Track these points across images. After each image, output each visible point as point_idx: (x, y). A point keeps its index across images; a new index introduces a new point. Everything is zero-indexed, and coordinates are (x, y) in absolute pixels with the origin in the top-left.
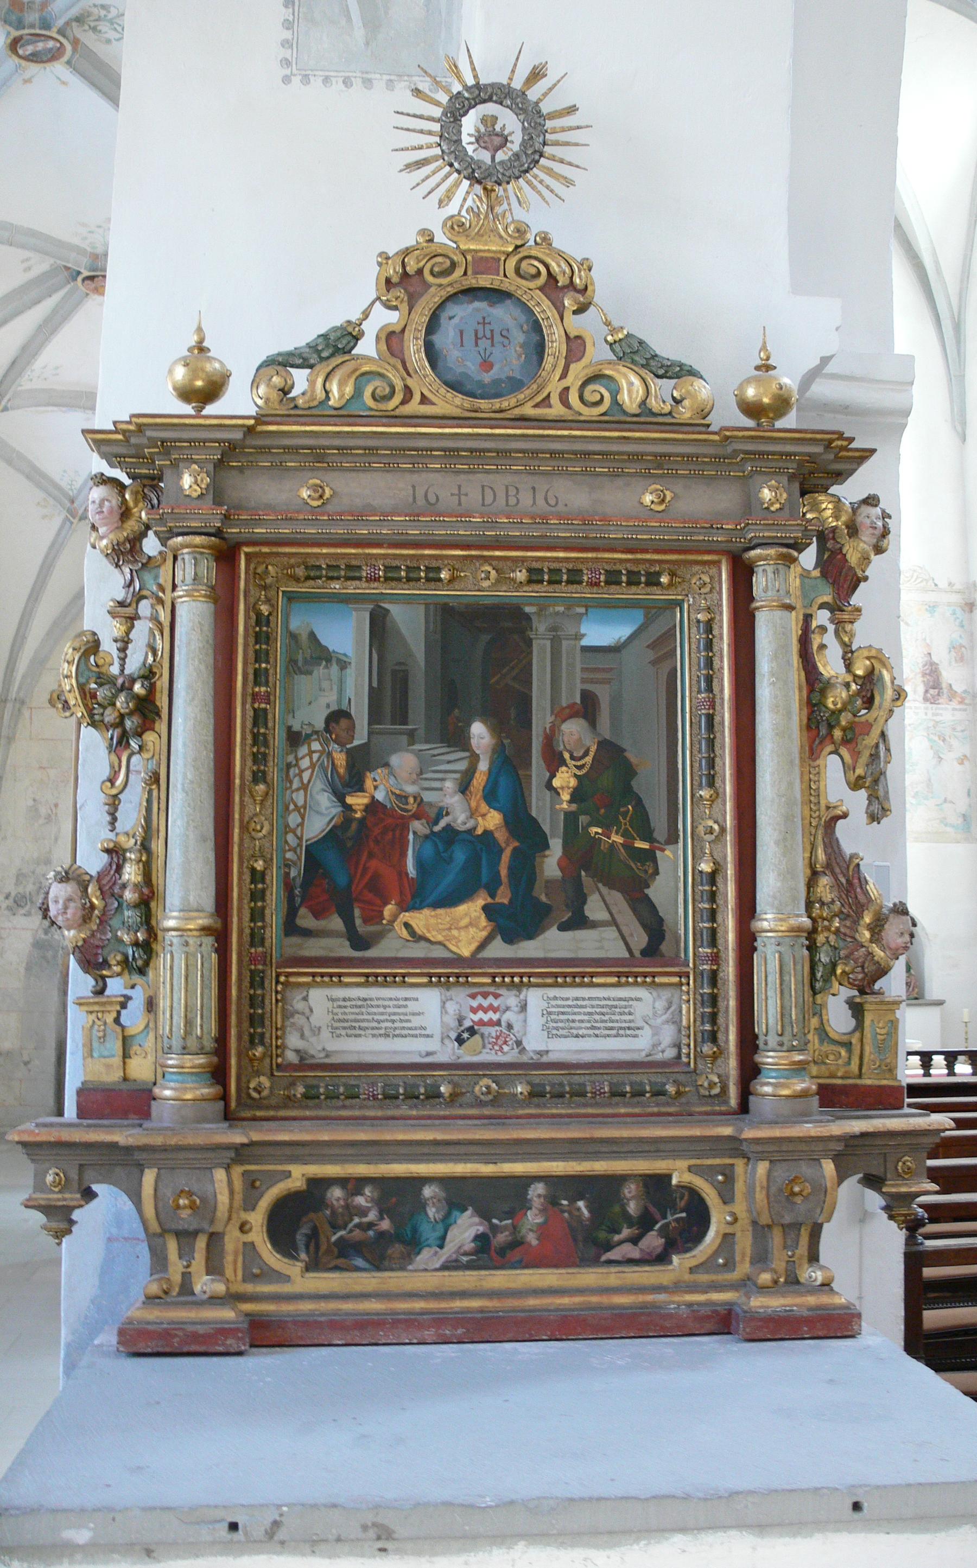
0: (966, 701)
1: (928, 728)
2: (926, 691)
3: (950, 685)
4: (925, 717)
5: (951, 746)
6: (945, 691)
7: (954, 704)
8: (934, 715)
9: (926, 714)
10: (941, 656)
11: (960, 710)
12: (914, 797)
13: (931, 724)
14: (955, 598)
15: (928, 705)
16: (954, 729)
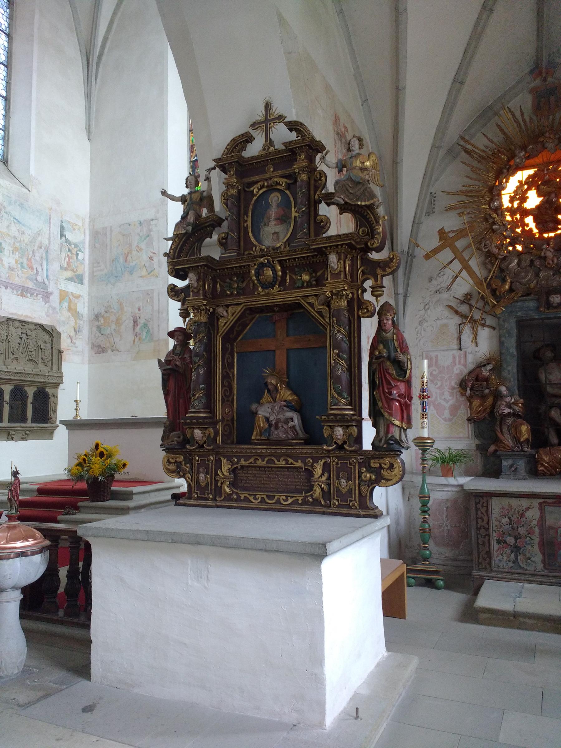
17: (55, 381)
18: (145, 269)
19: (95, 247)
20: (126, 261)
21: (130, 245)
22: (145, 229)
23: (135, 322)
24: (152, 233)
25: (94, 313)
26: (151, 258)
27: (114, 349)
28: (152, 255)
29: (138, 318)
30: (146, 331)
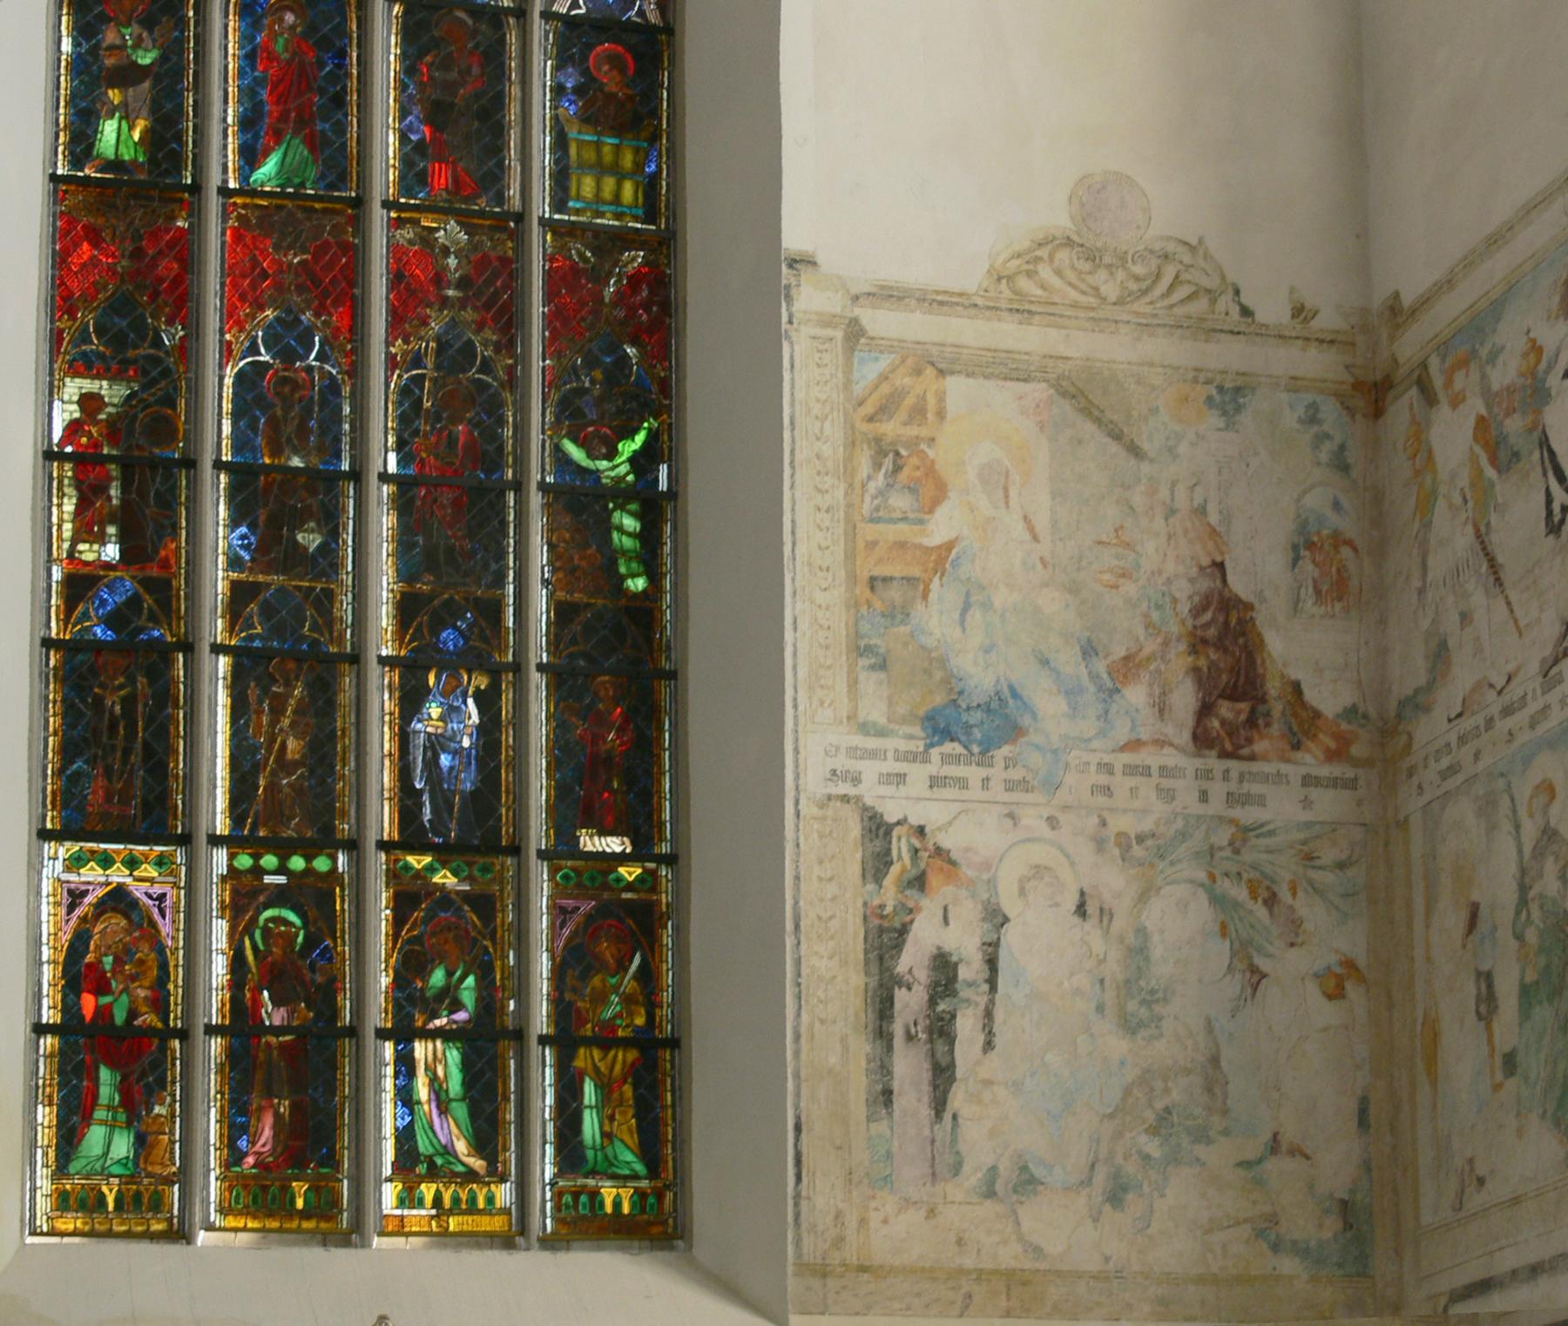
0: (1356, 750)
1: (1212, 851)
2: (1205, 710)
3: (1297, 688)
4: (1197, 809)
5: (1295, 924)
6: (1277, 708)
7: (1310, 761)
8: (1231, 799)
9: (1204, 797)
11: (1334, 783)
12: (1153, 1131)
13: (1223, 837)
14: (1316, 363)
15: (1212, 762)
16: (1309, 857)
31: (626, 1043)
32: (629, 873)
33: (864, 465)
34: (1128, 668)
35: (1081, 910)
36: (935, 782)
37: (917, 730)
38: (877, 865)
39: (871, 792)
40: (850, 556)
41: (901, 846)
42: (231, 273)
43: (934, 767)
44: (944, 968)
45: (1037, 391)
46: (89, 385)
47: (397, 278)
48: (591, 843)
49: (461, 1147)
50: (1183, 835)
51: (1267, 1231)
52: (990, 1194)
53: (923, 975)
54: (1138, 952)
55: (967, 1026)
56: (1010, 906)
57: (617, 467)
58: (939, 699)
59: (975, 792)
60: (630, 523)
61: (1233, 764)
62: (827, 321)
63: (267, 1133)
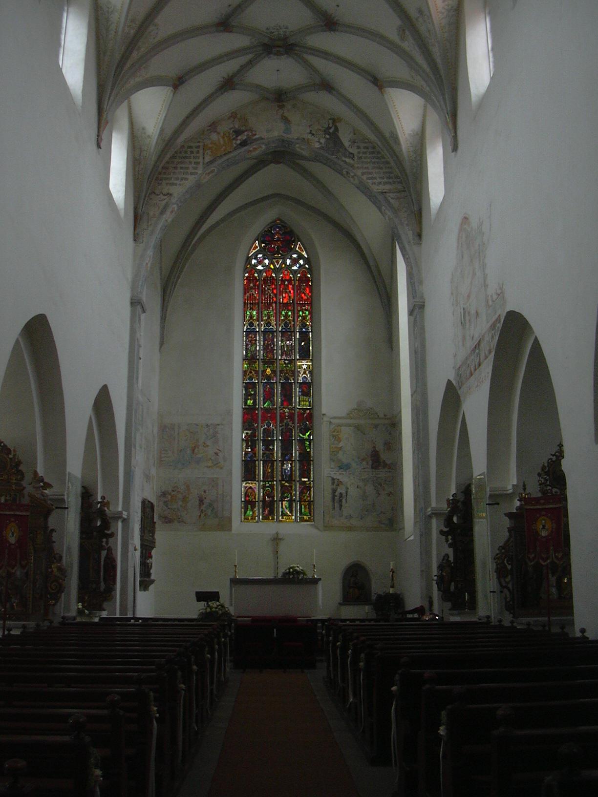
2: (373, 464)
3: (384, 461)
7: (386, 469)
10: (380, 447)
12: (366, 511)
13: (375, 478)
15: (374, 470)
17: (151, 545)
18: (210, 462)
19: (163, 438)
20: (193, 453)
21: (197, 440)
22: (211, 431)
23: (201, 501)
24: (218, 435)
25: (161, 491)
26: (216, 454)
27: (181, 521)
28: (218, 451)
29: (204, 498)
30: (211, 509)
31: (307, 501)
32: (308, 483)
33: (331, 438)
34: (363, 460)
35: (358, 487)
36: (340, 474)
37: (337, 468)
38: (333, 483)
39: (333, 475)
40: (330, 448)
41: (336, 481)
42: (262, 417)
43: (340, 472)
44: (341, 494)
45: (352, 428)
46: (247, 432)
47: (280, 416)
48: (303, 480)
49: (288, 513)
50: (370, 479)
51: (380, 522)
52: (347, 518)
53: (338, 495)
54: (365, 492)
55: (344, 501)
56: (349, 488)
57: (306, 437)
58: (340, 464)
59: (345, 475)
60: (308, 443)
61: (376, 470)
62: (327, 421)
63: (267, 511)
